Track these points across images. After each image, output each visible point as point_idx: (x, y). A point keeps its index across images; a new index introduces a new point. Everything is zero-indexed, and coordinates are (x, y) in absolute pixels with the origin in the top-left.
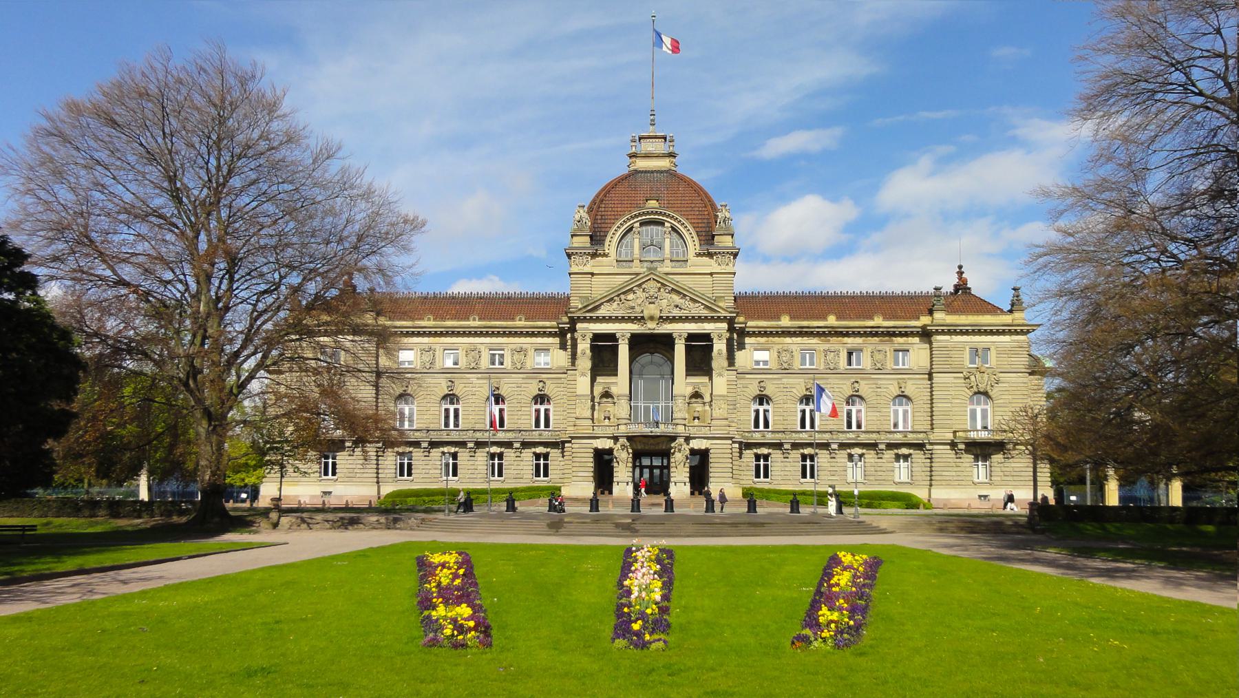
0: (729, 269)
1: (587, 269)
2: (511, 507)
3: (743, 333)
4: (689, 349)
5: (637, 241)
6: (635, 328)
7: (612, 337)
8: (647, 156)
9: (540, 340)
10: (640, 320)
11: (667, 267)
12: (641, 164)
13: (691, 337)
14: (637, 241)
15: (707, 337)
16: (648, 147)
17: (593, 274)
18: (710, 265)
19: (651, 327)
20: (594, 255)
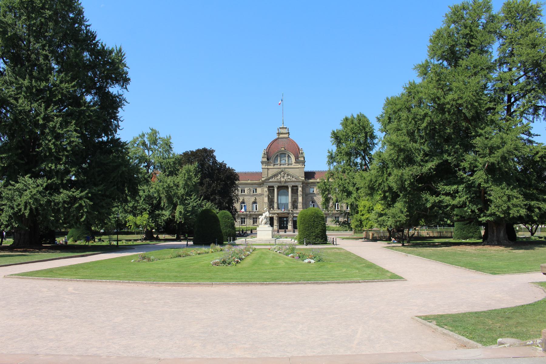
1: (266, 167)
2: (251, 232)
3: (307, 184)
4: (292, 189)
6: (279, 184)
7: (273, 187)
8: (282, 134)
9: (254, 186)
10: (280, 182)
11: (286, 166)
12: (281, 136)
13: (293, 186)
15: (297, 186)
16: (282, 131)
18: (299, 166)
19: (283, 184)
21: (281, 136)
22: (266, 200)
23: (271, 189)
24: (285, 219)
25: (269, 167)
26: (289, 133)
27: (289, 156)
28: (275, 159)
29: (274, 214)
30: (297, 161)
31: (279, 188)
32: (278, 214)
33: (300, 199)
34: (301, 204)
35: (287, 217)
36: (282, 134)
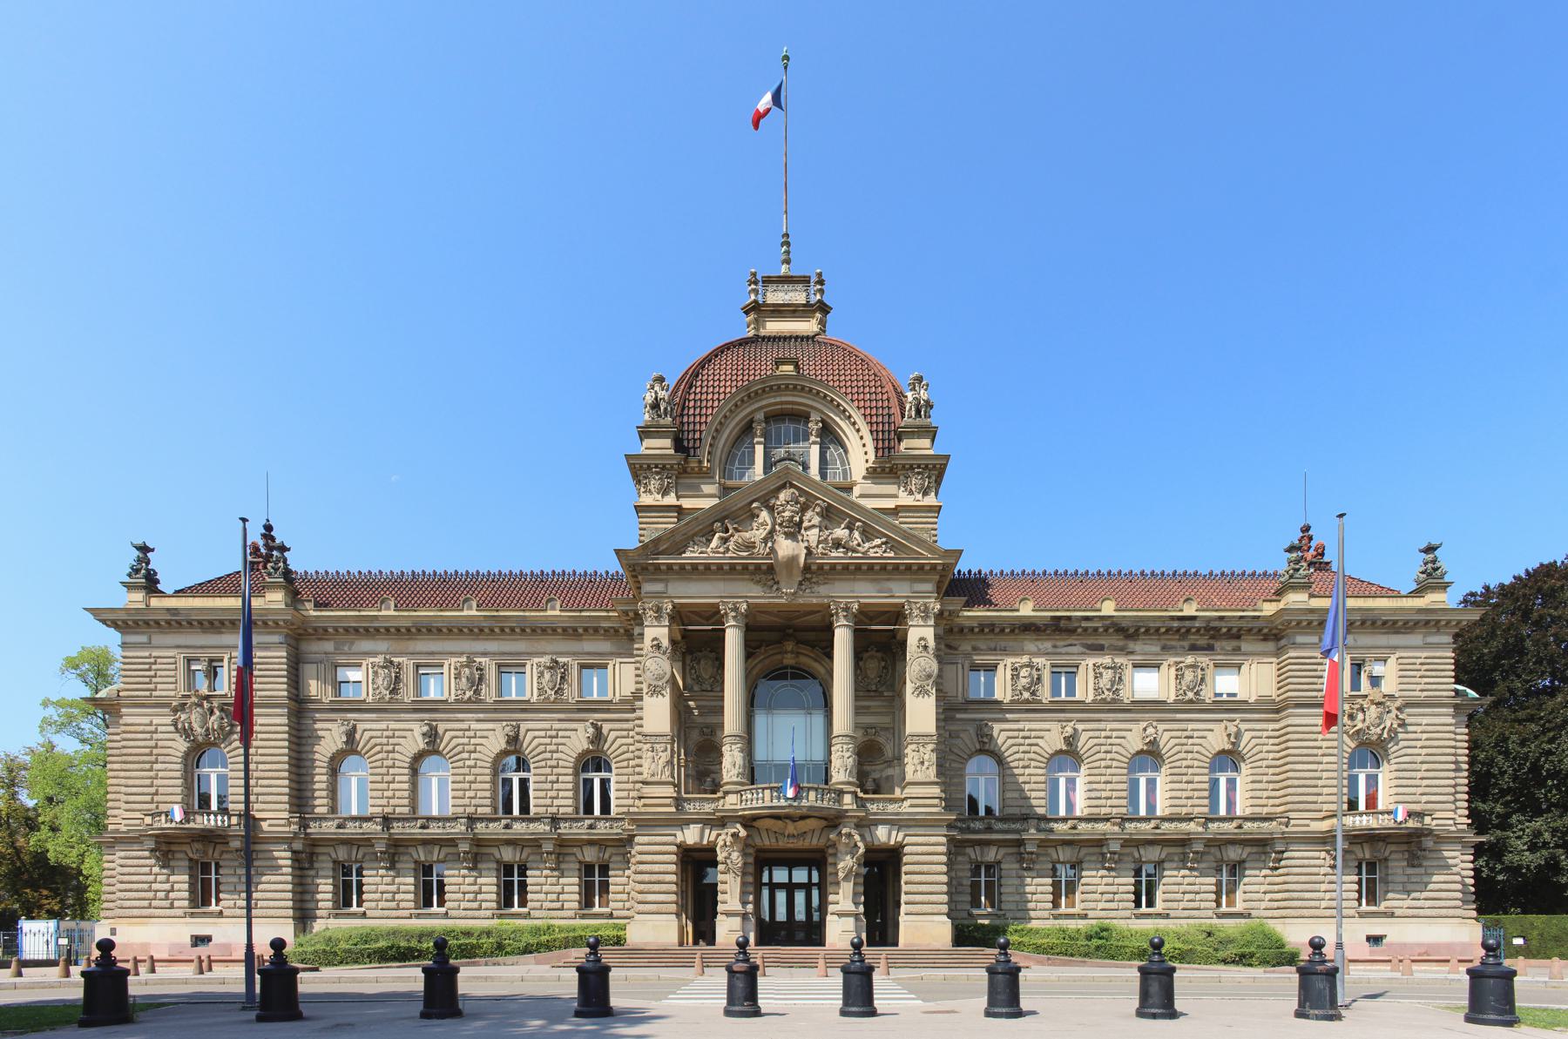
0: (931, 500)
1: (671, 500)
5: (759, 450)
8: (780, 311)
12: (774, 327)
14: (759, 450)
16: (776, 296)
17: (679, 510)
20: (683, 472)
21: (774, 327)
22: (657, 714)
23: (696, 645)
24: (800, 876)
25: (687, 503)
26: (824, 308)
27: (829, 435)
28: (729, 457)
29: (721, 822)
30: (888, 468)
31: (759, 635)
32: (749, 822)
33: (921, 713)
34: (929, 754)
35: (818, 860)
36: (780, 311)
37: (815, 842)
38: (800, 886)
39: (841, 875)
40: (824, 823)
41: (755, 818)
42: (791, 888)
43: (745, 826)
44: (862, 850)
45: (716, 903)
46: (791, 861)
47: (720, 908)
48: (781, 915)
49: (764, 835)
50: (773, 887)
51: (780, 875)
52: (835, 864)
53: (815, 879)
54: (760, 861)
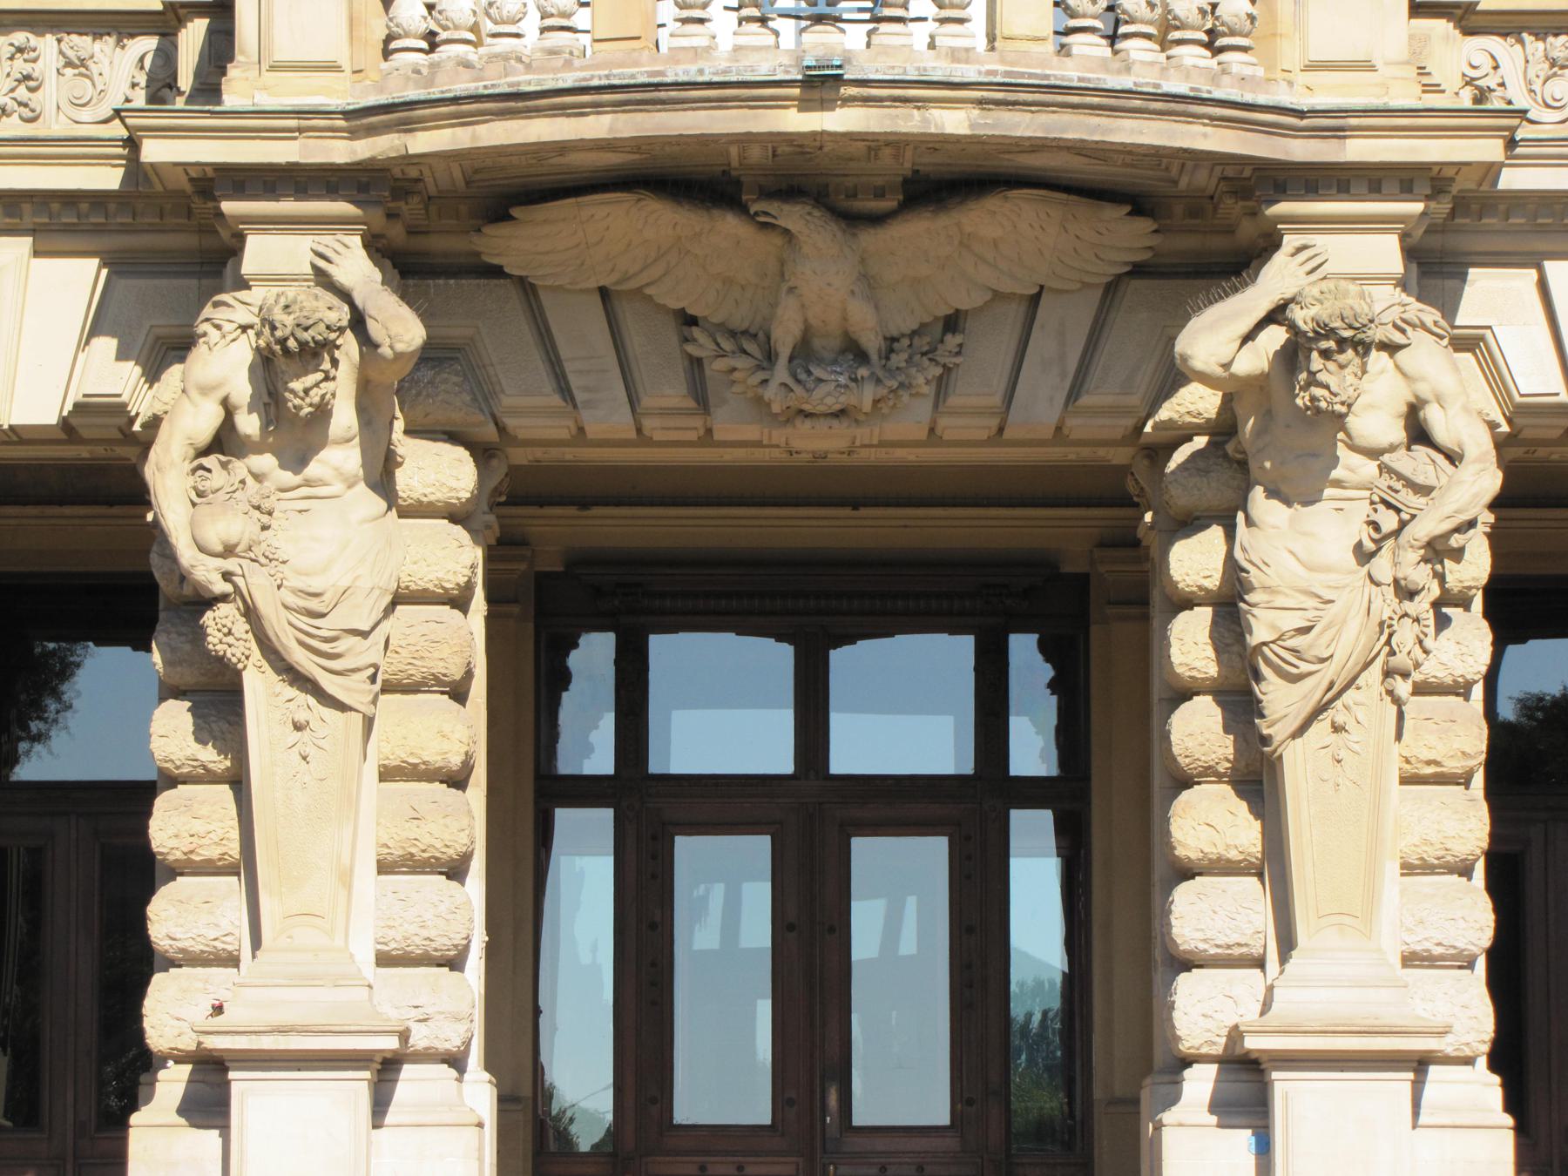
37: (1040, 405)
38: (899, 803)
39: (1281, 701)
40: (1128, 237)
41: (516, 189)
42: (812, 820)
43: (405, 266)
44: (1479, 482)
45: (132, 963)
46: (817, 604)
47: (171, 1013)
48: (726, 1071)
49: (582, 335)
50: (655, 813)
51: (722, 710)
52: (1229, 605)
53: (1031, 751)
54: (573, 584)
